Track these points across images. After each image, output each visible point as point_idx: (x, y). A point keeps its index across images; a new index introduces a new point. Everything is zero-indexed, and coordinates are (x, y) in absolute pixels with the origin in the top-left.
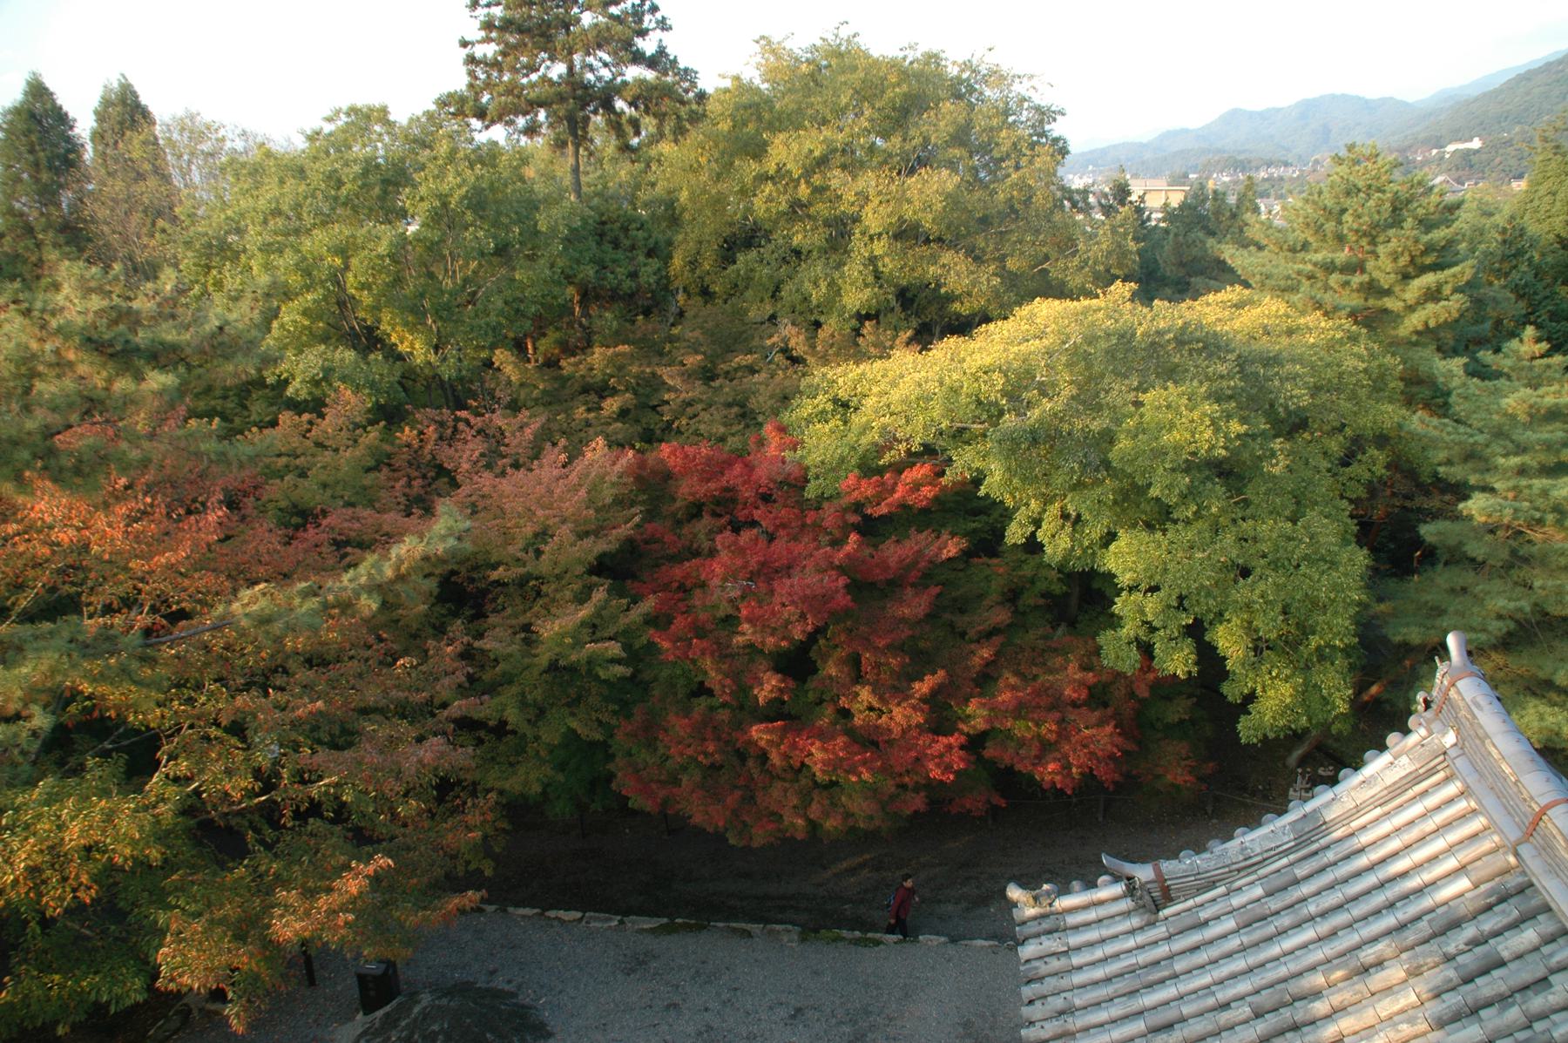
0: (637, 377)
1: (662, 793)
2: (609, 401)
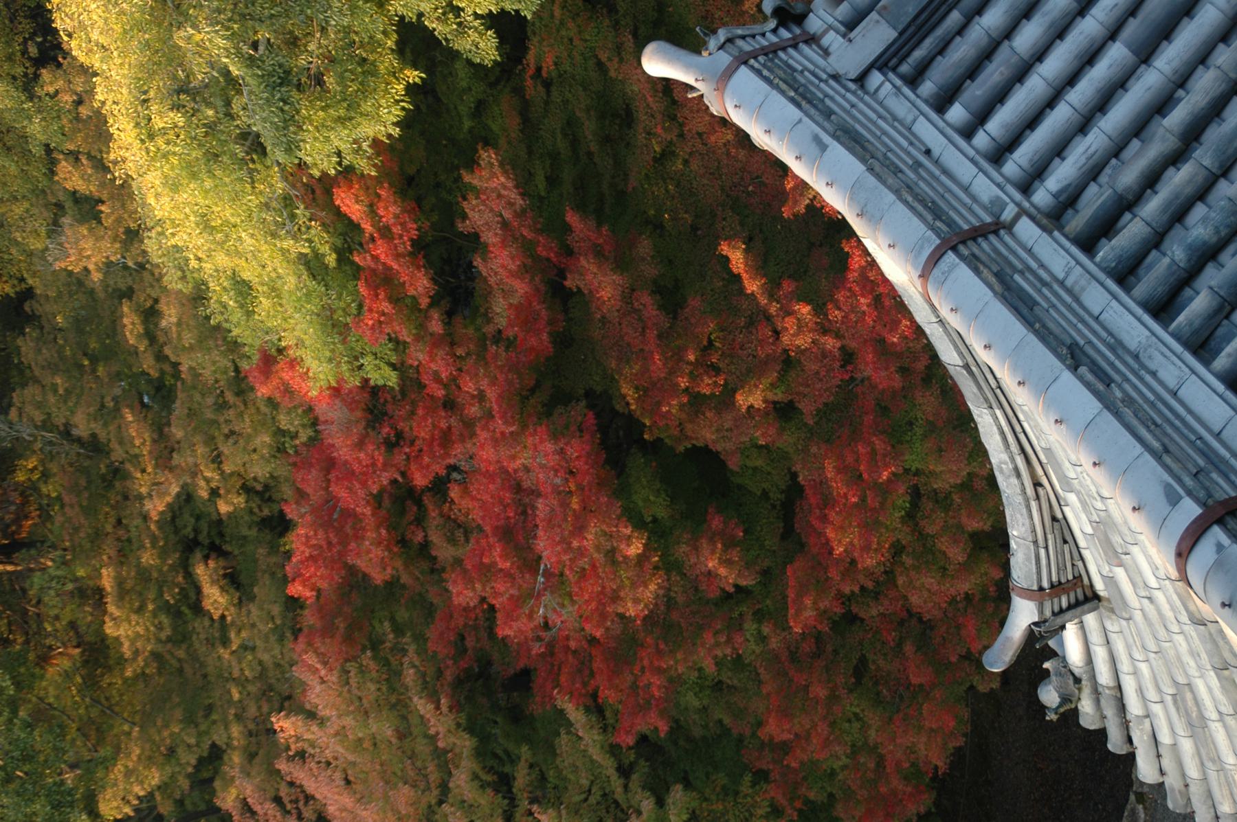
0: (163, 554)
1: (897, 783)
2: (207, 604)
